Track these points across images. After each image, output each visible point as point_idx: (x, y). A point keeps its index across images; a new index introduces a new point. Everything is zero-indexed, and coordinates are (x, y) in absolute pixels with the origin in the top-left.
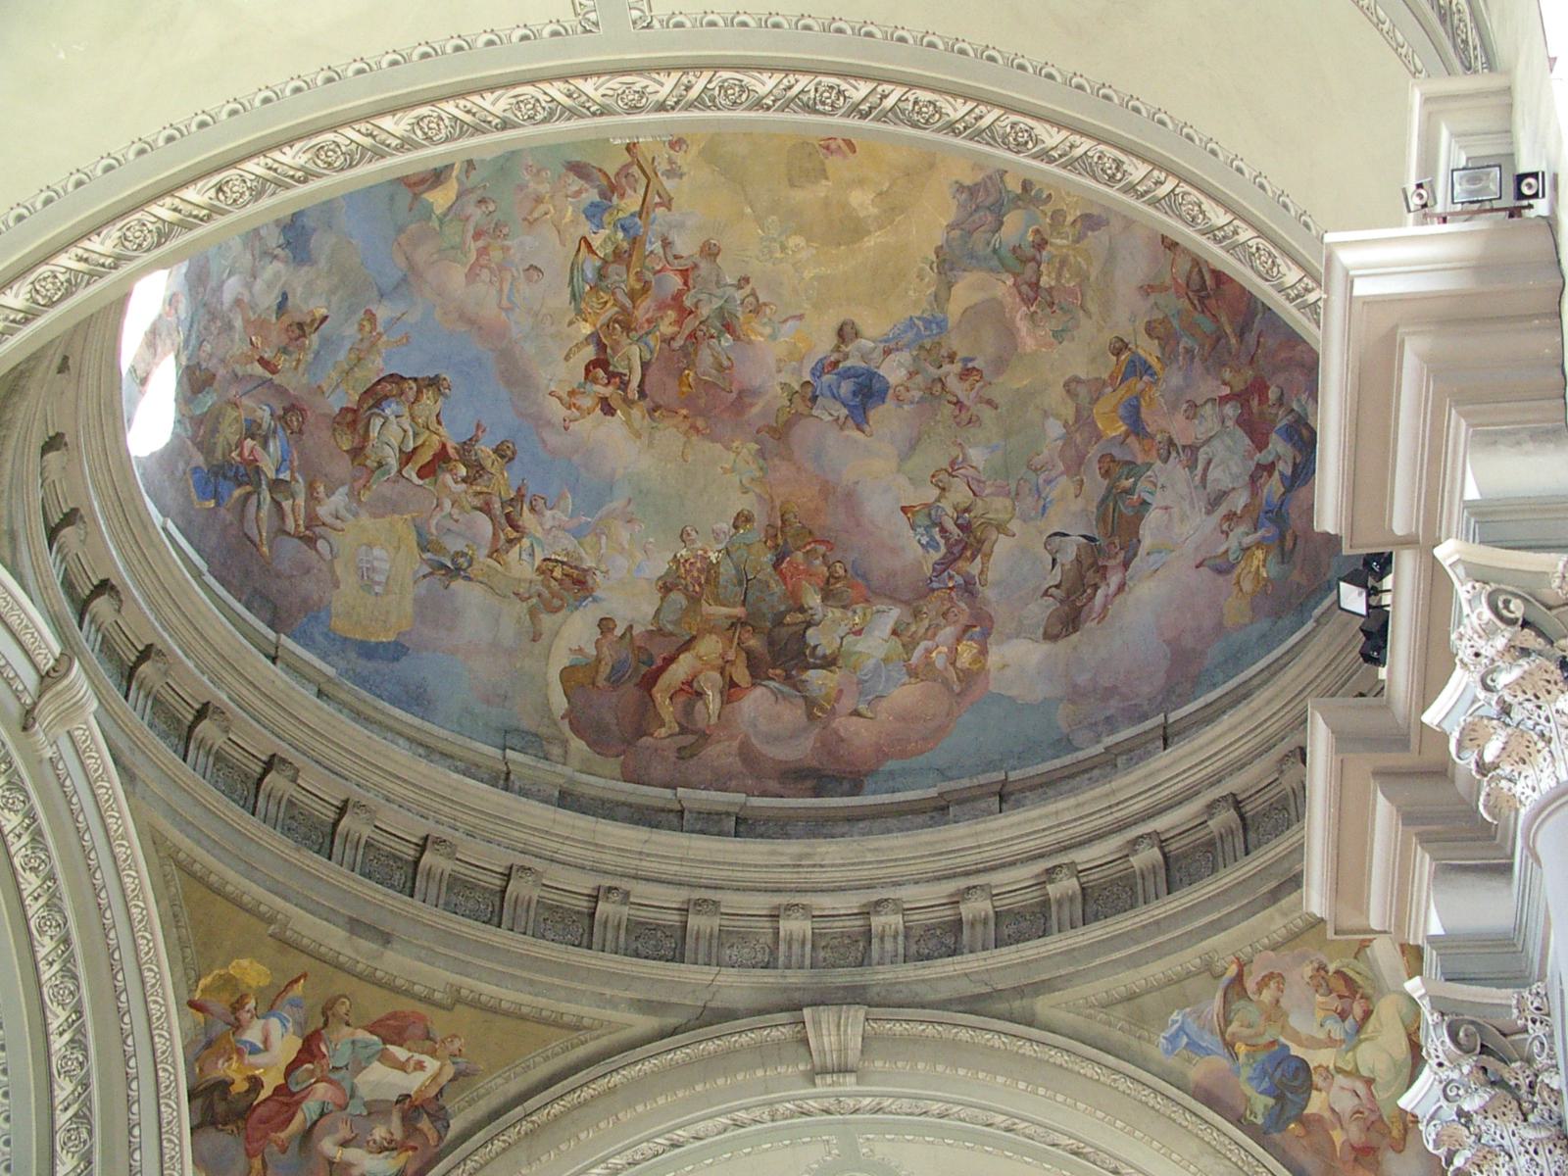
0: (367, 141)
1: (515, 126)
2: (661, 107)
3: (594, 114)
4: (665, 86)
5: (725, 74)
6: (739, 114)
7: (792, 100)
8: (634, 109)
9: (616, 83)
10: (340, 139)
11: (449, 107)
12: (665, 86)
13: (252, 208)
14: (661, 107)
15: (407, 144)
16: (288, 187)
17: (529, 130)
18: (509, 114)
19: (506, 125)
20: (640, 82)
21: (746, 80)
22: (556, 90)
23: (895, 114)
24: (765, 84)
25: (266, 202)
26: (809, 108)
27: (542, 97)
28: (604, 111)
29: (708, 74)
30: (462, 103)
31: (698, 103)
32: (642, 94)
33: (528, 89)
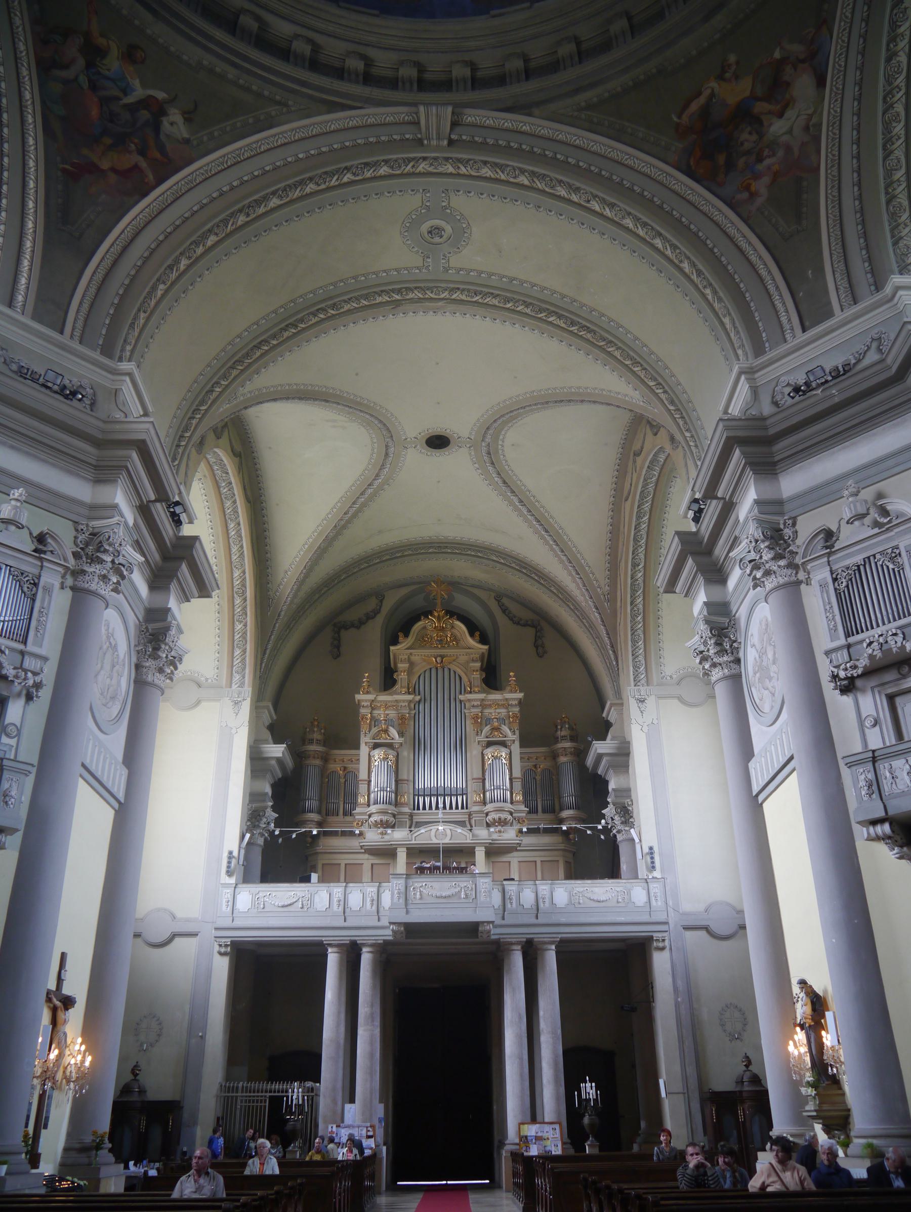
0: (535, 180)
1: (482, 161)
2: (425, 159)
3: (451, 158)
4: (422, 167)
5: (399, 172)
6: (394, 157)
7: (373, 166)
8: (435, 159)
9: (440, 170)
10: (544, 187)
11: (503, 177)
12: (422, 167)
13: (583, 186)
14: (425, 159)
15: (523, 171)
16: (568, 183)
17: (477, 158)
18: (483, 166)
19: (485, 163)
20: (431, 169)
21: (391, 171)
22: (463, 170)
23: (331, 174)
24: (384, 170)
25: (578, 184)
26: (366, 164)
27: (469, 169)
28: (447, 159)
29: (406, 171)
30: (498, 177)
31: (410, 160)
32: (431, 165)
33: (473, 173)
